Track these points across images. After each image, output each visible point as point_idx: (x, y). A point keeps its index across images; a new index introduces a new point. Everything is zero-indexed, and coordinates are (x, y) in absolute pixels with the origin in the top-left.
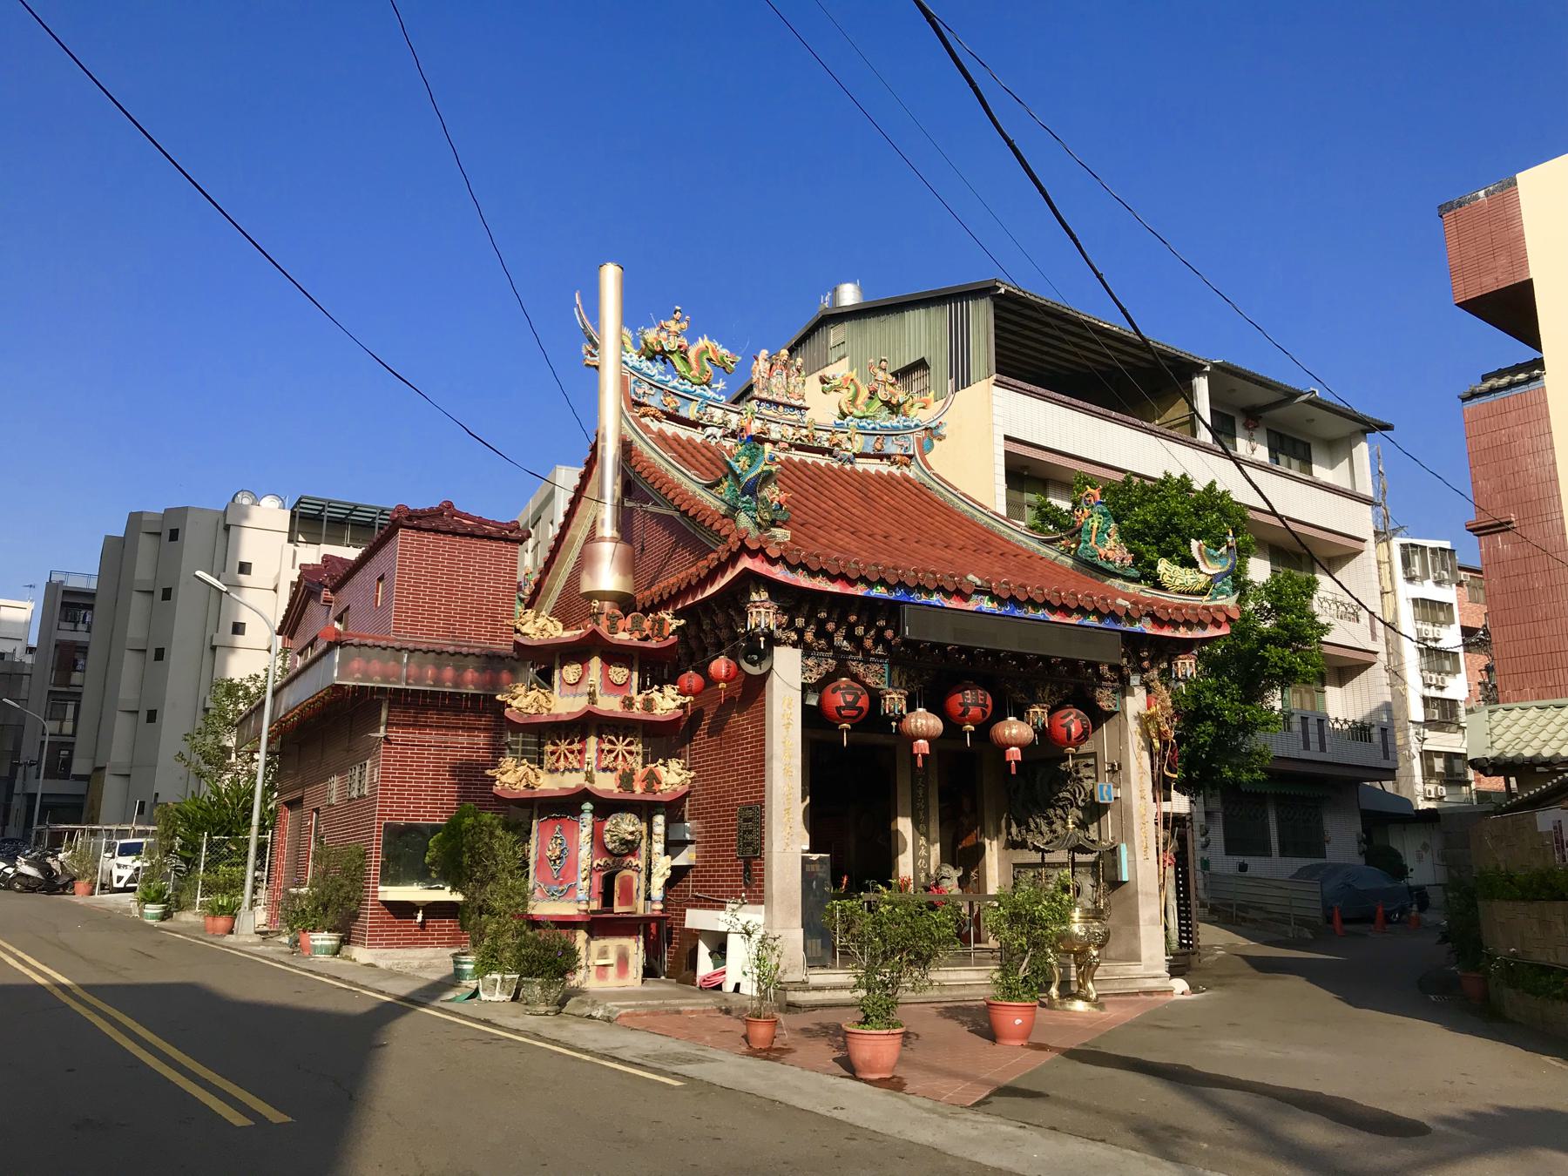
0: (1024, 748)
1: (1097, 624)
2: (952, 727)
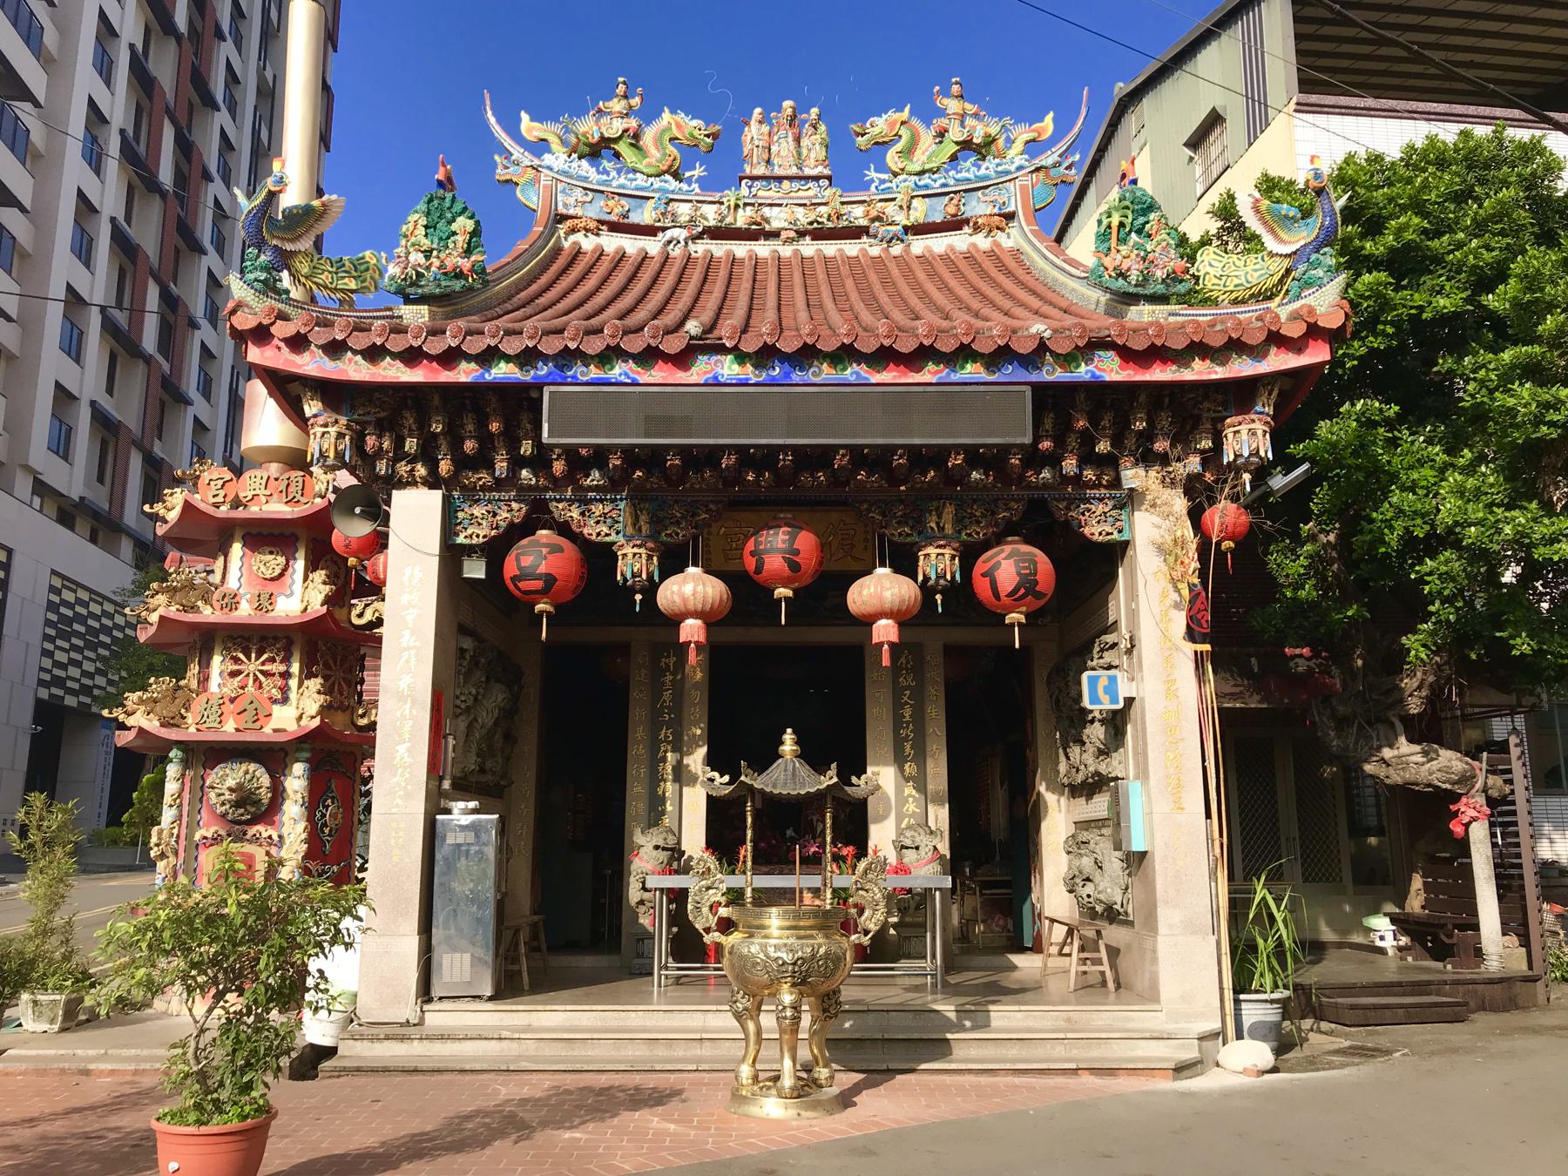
0: (904, 619)
1: (985, 376)
2: (747, 592)
